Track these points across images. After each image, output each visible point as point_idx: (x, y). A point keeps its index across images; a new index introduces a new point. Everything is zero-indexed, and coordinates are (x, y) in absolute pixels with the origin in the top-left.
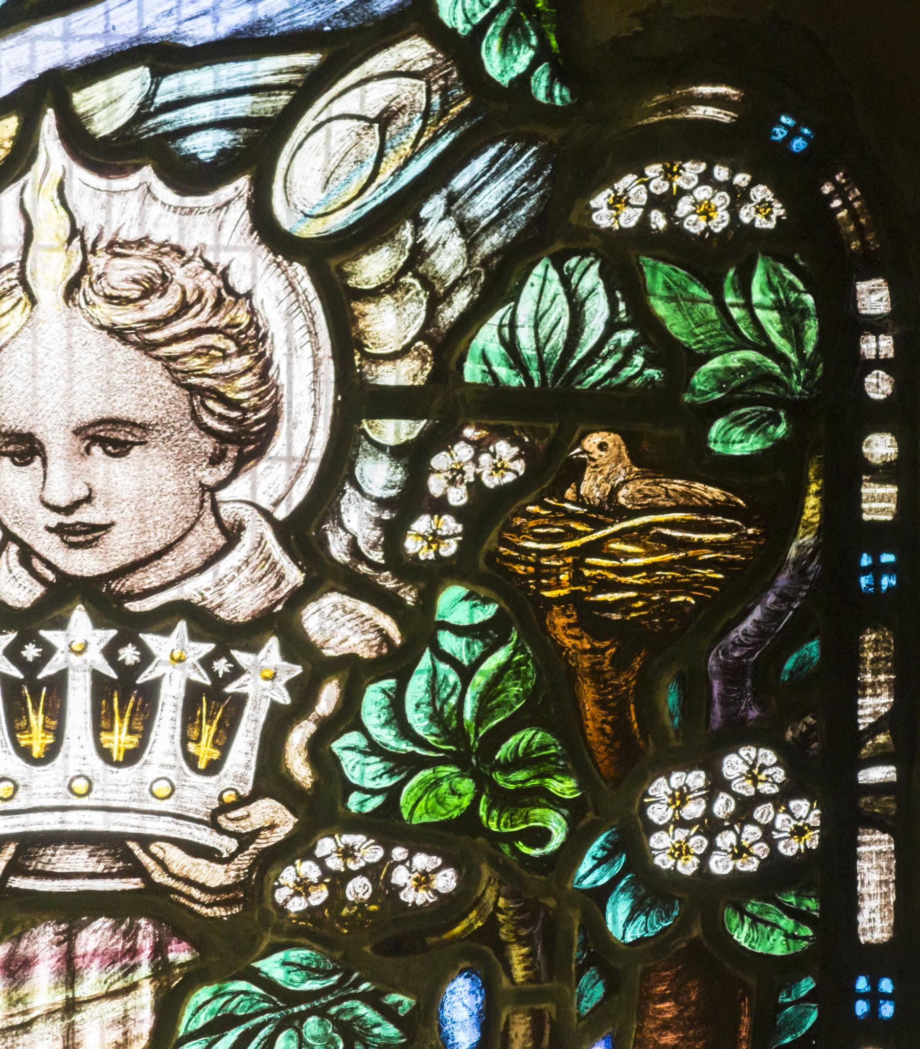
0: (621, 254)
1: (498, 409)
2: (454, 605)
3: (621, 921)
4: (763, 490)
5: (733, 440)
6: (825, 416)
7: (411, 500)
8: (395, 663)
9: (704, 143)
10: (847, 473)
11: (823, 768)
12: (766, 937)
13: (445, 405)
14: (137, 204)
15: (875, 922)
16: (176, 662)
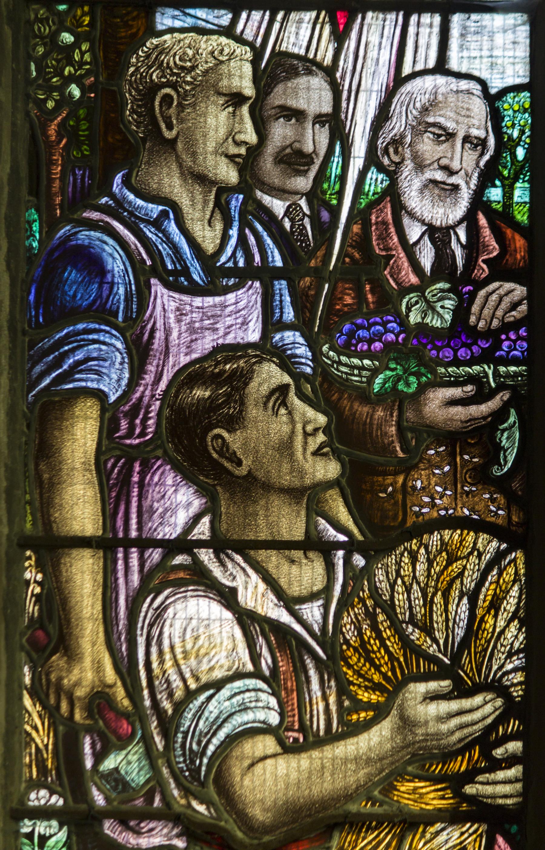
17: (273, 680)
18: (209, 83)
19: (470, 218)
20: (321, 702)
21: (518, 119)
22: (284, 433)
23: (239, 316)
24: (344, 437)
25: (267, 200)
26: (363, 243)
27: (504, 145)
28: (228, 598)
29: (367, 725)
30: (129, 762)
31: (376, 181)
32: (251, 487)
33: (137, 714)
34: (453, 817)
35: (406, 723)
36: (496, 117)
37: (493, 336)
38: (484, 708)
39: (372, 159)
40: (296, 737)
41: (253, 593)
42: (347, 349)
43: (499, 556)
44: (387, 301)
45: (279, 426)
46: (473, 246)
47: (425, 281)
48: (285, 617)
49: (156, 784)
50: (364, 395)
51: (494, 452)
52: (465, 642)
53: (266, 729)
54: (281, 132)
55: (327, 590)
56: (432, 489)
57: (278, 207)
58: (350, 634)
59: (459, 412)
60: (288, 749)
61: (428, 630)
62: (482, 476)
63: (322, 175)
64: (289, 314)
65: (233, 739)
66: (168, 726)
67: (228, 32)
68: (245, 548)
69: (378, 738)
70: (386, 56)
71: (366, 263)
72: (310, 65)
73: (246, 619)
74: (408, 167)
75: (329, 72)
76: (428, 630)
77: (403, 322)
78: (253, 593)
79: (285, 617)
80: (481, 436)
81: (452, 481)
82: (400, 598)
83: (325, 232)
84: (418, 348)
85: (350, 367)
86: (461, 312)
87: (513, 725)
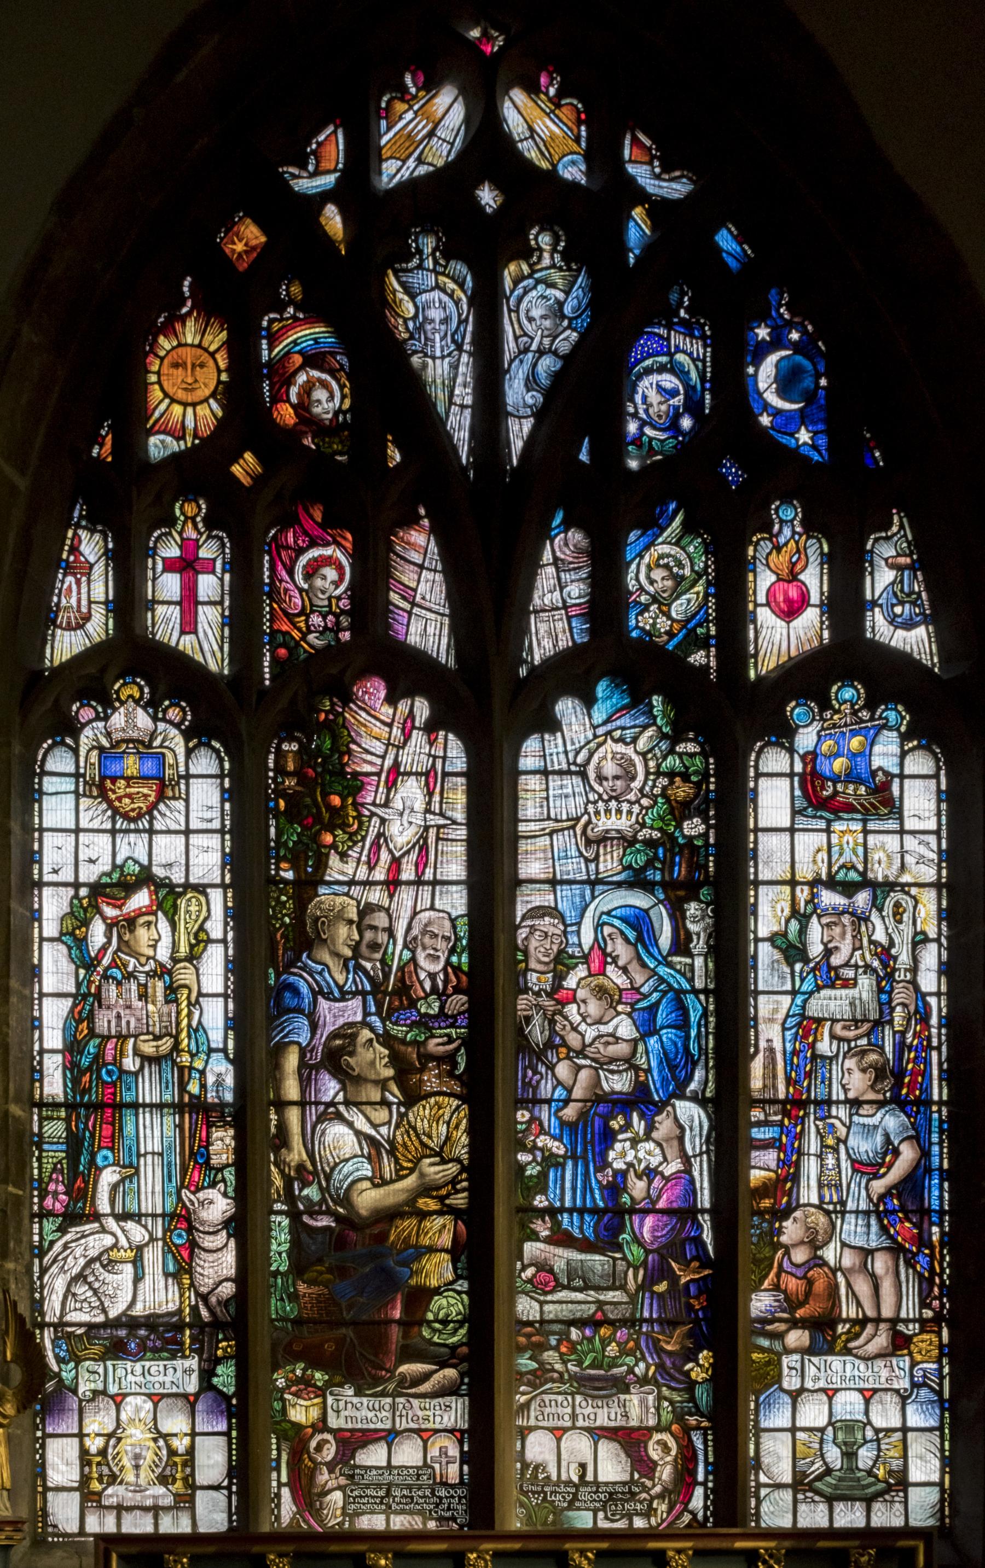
0: (680, 755)
1: (665, 774)
2: (660, 800)
3: (681, 841)
4: (698, 785)
5: (694, 779)
6: (705, 776)
7: (654, 786)
8: (652, 807)
9: (691, 740)
10: (708, 783)
11: (705, 820)
12: (699, 843)
13: (658, 774)
14: (620, 748)
15: (712, 841)
16: (625, 807)
17: (369, 1158)
18: (340, 916)
19: (445, 969)
20: (388, 1168)
21: (463, 931)
22: (372, 1058)
23: (353, 1010)
24: (396, 1059)
25: (363, 963)
26: (401, 980)
27: (458, 939)
28: (350, 1125)
29: (406, 1176)
30: (312, 1192)
31: (407, 955)
32: (359, 1080)
33: (315, 1173)
34: (440, 1213)
35: (422, 1175)
36: (454, 927)
37: (454, 1017)
38: (453, 1168)
39: (405, 946)
40: (378, 1181)
41: (361, 1123)
42: (396, 1023)
43: (458, 1107)
44: (413, 1004)
45: (369, 1055)
46: (446, 981)
47: (427, 995)
48: (373, 1133)
49: (323, 1200)
50: (403, 1041)
51: (455, 1065)
52: (445, 1143)
53: (367, 1178)
54: (369, 935)
55: (389, 1122)
56: (431, 1080)
57: (368, 965)
58: (399, 1139)
59: (441, 1048)
60: (376, 1186)
61: (430, 1137)
62: (451, 1074)
63: (385, 953)
64: (373, 1009)
65: (354, 1182)
66: (328, 1178)
67: (347, 894)
68: (357, 1104)
69: (411, 1181)
70: (410, 904)
71: (403, 989)
72: (380, 908)
73: (358, 1133)
74: (419, 950)
75: (387, 910)
76: (430, 1137)
77: (419, 1011)
78: (361, 1123)
79: (373, 1133)
80: (450, 1058)
81: (439, 1076)
82: (419, 1124)
83: (386, 976)
84: (424, 1023)
85: (398, 1031)
86: (442, 1008)
87: (464, 1176)
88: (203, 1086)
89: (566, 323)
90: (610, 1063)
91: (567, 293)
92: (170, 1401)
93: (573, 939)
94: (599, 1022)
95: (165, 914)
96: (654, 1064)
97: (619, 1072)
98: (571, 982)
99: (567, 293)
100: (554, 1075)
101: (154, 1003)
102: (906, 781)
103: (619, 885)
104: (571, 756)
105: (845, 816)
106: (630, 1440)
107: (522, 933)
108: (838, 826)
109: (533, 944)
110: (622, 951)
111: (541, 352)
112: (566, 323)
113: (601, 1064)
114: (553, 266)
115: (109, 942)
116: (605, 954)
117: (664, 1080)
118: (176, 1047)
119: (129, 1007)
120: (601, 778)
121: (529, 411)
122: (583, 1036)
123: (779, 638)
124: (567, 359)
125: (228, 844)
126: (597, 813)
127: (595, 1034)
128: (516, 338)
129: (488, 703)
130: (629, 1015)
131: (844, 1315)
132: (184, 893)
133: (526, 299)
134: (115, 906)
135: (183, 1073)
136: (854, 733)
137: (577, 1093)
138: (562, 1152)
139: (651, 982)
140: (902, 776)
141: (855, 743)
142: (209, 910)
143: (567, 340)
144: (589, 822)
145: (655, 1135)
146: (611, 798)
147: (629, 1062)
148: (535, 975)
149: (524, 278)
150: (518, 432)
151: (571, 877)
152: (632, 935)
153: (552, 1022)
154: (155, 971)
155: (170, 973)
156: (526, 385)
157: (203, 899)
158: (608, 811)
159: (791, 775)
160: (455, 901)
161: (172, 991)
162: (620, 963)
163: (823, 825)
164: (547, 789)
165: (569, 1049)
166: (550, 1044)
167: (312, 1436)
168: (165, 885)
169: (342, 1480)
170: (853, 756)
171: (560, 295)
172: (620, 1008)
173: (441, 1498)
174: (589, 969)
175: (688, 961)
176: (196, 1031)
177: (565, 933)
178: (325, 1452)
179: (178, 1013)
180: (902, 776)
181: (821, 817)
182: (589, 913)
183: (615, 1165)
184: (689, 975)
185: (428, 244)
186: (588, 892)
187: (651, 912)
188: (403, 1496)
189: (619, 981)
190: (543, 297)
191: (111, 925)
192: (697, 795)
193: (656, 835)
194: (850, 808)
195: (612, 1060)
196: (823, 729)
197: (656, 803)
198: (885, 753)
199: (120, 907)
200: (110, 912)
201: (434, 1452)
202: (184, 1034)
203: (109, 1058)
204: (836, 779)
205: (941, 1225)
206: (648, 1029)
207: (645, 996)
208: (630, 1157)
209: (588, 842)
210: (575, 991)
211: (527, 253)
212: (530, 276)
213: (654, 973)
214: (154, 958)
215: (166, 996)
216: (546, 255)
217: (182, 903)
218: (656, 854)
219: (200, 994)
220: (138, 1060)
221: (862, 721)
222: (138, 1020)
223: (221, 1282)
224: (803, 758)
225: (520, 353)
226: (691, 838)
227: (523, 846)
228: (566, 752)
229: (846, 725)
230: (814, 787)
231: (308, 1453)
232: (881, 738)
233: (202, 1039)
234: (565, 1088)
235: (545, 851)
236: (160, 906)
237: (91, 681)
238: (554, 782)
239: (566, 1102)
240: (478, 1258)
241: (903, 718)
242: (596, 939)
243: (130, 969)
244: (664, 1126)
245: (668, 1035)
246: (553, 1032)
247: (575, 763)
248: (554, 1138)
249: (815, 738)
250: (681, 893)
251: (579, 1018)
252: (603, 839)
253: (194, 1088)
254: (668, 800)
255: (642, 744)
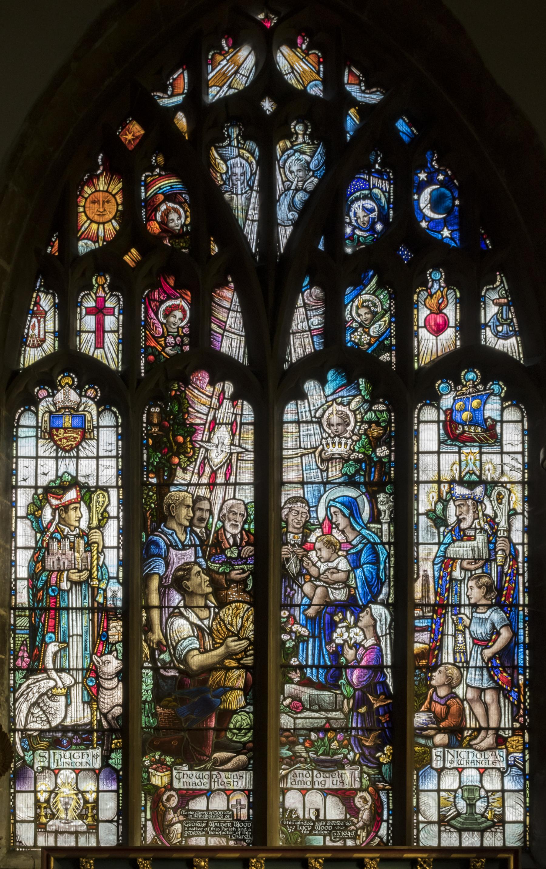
0: (375, 412)
1: (366, 422)
2: (363, 437)
3: (375, 459)
4: (385, 428)
5: (383, 424)
6: (389, 422)
7: (360, 429)
8: (359, 441)
9: (381, 403)
10: (391, 427)
11: (389, 448)
12: (385, 460)
13: (362, 422)
14: (341, 408)
15: (393, 459)
16: (343, 441)
17: (198, 637)
18: (182, 503)
19: (241, 532)
20: (208, 643)
21: (251, 510)
22: (200, 582)
23: (189, 555)
24: (213, 582)
25: (195, 529)
26: (216, 538)
27: (249, 515)
28: (187, 619)
29: (218, 648)
30: (166, 657)
31: (220, 524)
32: (192, 594)
33: (167, 646)
34: (237, 668)
35: (227, 647)
36: (246, 509)
37: (246, 558)
38: (245, 643)
39: (219, 519)
40: (203, 650)
41: (193, 618)
42: (213, 562)
43: (248, 609)
44: (223, 551)
45: (198, 580)
46: (242, 539)
47: (231, 547)
48: (200, 623)
49: (172, 661)
50: (217, 572)
51: (246, 585)
52: (241, 629)
53: (196, 649)
54: (198, 514)
55: (209, 618)
56: (233, 594)
57: (198, 530)
58: (215, 627)
59: (239, 576)
60: (201, 653)
61: (232, 626)
62: (244, 591)
63: (207, 523)
64: (201, 555)
65: (189, 651)
66: (175, 648)
67: (186, 491)
68: (191, 607)
69: (221, 650)
70: (222, 496)
71: (218, 543)
72: (205, 498)
73: (192, 624)
74: (227, 521)
75: (209, 500)
76: (232, 626)
77: (226, 556)
78: (193, 618)
79: (200, 623)
80: (244, 582)
81: (237, 592)
82: (226, 618)
83: (208, 536)
84: (229, 562)
85: (214, 566)
86: (239, 554)
87: (251, 647)
88: (105, 598)
89: (311, 173)
90: (334, 584)
91: (312, 157)
92: (85, 773)
93: (314, 515)
94: (328, 561)
95: (85, 503)
96: (359, 584)
97: (340, 589)
98: (312, 539)
99: (312, 157)
100: (302, 590)
101: (78, 552)
102: (505, 424)
103: (340, 484)
104: (313, 413)
105: (469, 444)
106: (345, 796)
107: (285, 512)
108: (465, 450)
109: (291, 517)
110: (341, 521)
111: (297, 190)
112: (311, 173)
113: (329, 584)
114: (304, 142)
115: (54, 519)
116: (332, 523)
117: (365, 594)
118: (90, 576)
119: (65, 554)
120: (330, 425)
121: (290, 222)
122: (319, 569)
123: (431, 345)
124: (312, 193)
125: (120, 464)
126: (328, 444)
127: (325, 568)
128: (283, 183)
129: (267, 385)
130: (345, 557)
131: (468, 726)
132: (96, 491)
133: (289, 161)
134: (57, 499)
135: (94, 591)
136: (474, 398)
137: (316, 601)
138: (307, 634)
139: (358, 538)
140: (502, 422)
141: (475, 403)
142: (109, 501)
143: (312, 183)
144: (323, 449)
145: (360, 624)
146: (335, 436)
147: (345, 583)
148: (292, 535)
149: (288, 149)
150: (284, 234)
151: (313, 480)
152: (347, 512)
153: (301, 561)
154: (79, 535)
155: (87, 535)
156: (289, 208)
157: (106, 494)
158: (334, 443)
159: (438, 422)
160: (247, 494)
161: (88, 545)
162: (340, 528)
163: (456, 449)
164: (299, 432)
165: (311, 576)
166: (300, 574)
167: (165, 793)
168: (85, 487)
169: (181, 818)
170: (474, 410)
171: (308, 158)
172: (340, 553)
173: (237, 828)
174: (322, 531)
175: (379, 526)
176: (102, 567)
177: (309, 511)
178: (171, 802)
179: (92, 557)
180: (502, 422)
181: (455, 445)
182: (323, 500)
183: (337, 641)
184: (379, 534)
185: (234, 132)
186: (322, 489)
187: (358, 499)
188: (216, 827)
189: (339, 538)
190: (298, 159)
191: (55, 509)
192: (384, 434)
193: (361, 456)
194: (472, 440)
195: (335, 582)
196: (456, 396)
197: (361, 438)
198: (492, 410)
199: (60, 499)
200: (54, 502)
201: (233, 802)
202: (95, 569)
203: (53, 583)
204: (464, 424)
205: (524, 675)
206: (356, 565)
207: (354, 547)
208: (345, 637)
209: (323, 461)
210: (314, 544)
211: (289, 135)
212: (291, 148)
213: (359, 533)
214: (78, 527)
215: (85, 548)
216: (300, 137)
217: (94, 497)
218: (361, 467)
219: (104, 547)
220: (69, 584)
221: (479, 391)
222: (69, 561)
223: (114, 707)
224: (445, 412)
225: (285, 190)
226: (380, 458)
227: (285, 463)
228: (310, 411)
229: (470, 393)
230: (451, 429)
231: (162, 802)
232: (490, 400)
233: (105, 572)
234: (308, 598)
235: (298, 466)
236: (82, 499)
237: (47, 374)
238: (303, 427)
239: (309, 606)
240: (258, 693)
241: (503, 389)
242: (327, 515)
243: (65, 533)
244: (365, 619)
245: (367, 568)
246: (302, 567)
247: (315, 417)
248: (302, 626)
249: (452, 401)
250: (375, 488)
251: (317, 559)
252: (331, 459)
253: (100, 599)
254: (368, 437)
255: (353, 405)
